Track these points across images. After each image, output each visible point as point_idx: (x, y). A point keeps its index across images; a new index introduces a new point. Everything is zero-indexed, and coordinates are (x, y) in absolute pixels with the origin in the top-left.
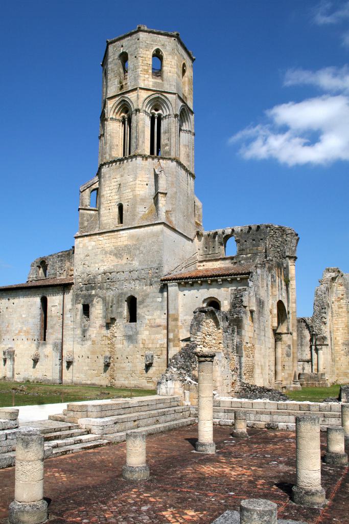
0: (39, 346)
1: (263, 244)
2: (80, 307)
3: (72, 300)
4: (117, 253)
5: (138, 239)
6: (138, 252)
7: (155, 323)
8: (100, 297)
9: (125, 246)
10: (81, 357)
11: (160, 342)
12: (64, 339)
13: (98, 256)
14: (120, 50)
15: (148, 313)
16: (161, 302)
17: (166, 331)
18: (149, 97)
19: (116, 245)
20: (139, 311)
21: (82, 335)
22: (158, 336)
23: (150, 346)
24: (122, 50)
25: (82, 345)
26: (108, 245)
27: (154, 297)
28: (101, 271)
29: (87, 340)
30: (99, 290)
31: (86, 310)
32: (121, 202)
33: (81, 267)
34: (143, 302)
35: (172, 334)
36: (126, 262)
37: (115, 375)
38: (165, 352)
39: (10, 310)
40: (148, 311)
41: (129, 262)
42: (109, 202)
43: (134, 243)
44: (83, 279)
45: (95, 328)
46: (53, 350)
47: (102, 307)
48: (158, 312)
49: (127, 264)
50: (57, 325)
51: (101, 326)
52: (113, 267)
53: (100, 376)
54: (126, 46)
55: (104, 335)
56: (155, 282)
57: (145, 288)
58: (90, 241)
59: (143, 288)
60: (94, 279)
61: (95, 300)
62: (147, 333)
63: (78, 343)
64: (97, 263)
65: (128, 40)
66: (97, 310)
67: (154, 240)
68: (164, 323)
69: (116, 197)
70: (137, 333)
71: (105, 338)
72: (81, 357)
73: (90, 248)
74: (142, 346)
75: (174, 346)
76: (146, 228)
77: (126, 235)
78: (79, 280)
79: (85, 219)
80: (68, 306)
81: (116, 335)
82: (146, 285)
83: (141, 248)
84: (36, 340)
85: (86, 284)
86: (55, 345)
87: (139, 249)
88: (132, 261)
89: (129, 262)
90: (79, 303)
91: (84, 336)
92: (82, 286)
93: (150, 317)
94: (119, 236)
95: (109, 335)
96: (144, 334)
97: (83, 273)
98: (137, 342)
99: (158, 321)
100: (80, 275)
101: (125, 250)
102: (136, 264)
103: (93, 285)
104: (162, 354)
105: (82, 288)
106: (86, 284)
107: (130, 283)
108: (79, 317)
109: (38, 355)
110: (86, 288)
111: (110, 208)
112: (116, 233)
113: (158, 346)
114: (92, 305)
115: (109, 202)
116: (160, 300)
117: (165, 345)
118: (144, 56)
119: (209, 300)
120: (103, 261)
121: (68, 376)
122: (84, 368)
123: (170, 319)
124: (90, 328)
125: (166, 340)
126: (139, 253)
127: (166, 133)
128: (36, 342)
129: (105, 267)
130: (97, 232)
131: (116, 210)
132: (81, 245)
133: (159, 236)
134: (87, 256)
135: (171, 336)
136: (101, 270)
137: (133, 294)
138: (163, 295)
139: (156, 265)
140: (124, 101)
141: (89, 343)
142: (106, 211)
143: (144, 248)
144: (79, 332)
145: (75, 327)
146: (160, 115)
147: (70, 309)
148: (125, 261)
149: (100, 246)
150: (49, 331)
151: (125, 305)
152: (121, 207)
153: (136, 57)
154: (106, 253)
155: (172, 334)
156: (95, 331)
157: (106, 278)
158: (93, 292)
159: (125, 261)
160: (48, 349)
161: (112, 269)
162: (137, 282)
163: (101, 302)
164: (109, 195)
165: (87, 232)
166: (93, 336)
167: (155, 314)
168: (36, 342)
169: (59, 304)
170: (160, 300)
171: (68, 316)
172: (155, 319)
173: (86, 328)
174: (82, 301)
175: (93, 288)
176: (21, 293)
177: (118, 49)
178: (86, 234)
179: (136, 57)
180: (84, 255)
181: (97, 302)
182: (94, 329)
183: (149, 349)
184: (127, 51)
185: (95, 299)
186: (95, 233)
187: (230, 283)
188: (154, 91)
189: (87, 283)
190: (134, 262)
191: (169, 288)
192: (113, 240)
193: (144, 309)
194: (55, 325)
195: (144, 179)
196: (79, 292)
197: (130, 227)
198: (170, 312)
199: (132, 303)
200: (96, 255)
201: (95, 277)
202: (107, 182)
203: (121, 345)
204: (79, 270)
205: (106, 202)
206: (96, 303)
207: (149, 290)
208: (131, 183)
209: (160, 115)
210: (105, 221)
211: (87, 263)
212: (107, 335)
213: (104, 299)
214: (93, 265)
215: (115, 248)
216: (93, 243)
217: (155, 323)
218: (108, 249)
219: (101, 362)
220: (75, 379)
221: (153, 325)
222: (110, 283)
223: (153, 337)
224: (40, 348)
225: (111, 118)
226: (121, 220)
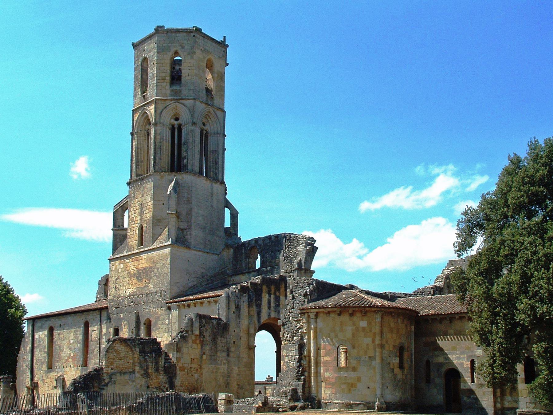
4: (140, 275)
27: (164, 319)
39: (62, 336)
83: (156, 271)
128: (80, 368)
134: (118, 278)
150: (90, 356)
151: (143, 328)
168: (80, 368)
216: (122, 266)
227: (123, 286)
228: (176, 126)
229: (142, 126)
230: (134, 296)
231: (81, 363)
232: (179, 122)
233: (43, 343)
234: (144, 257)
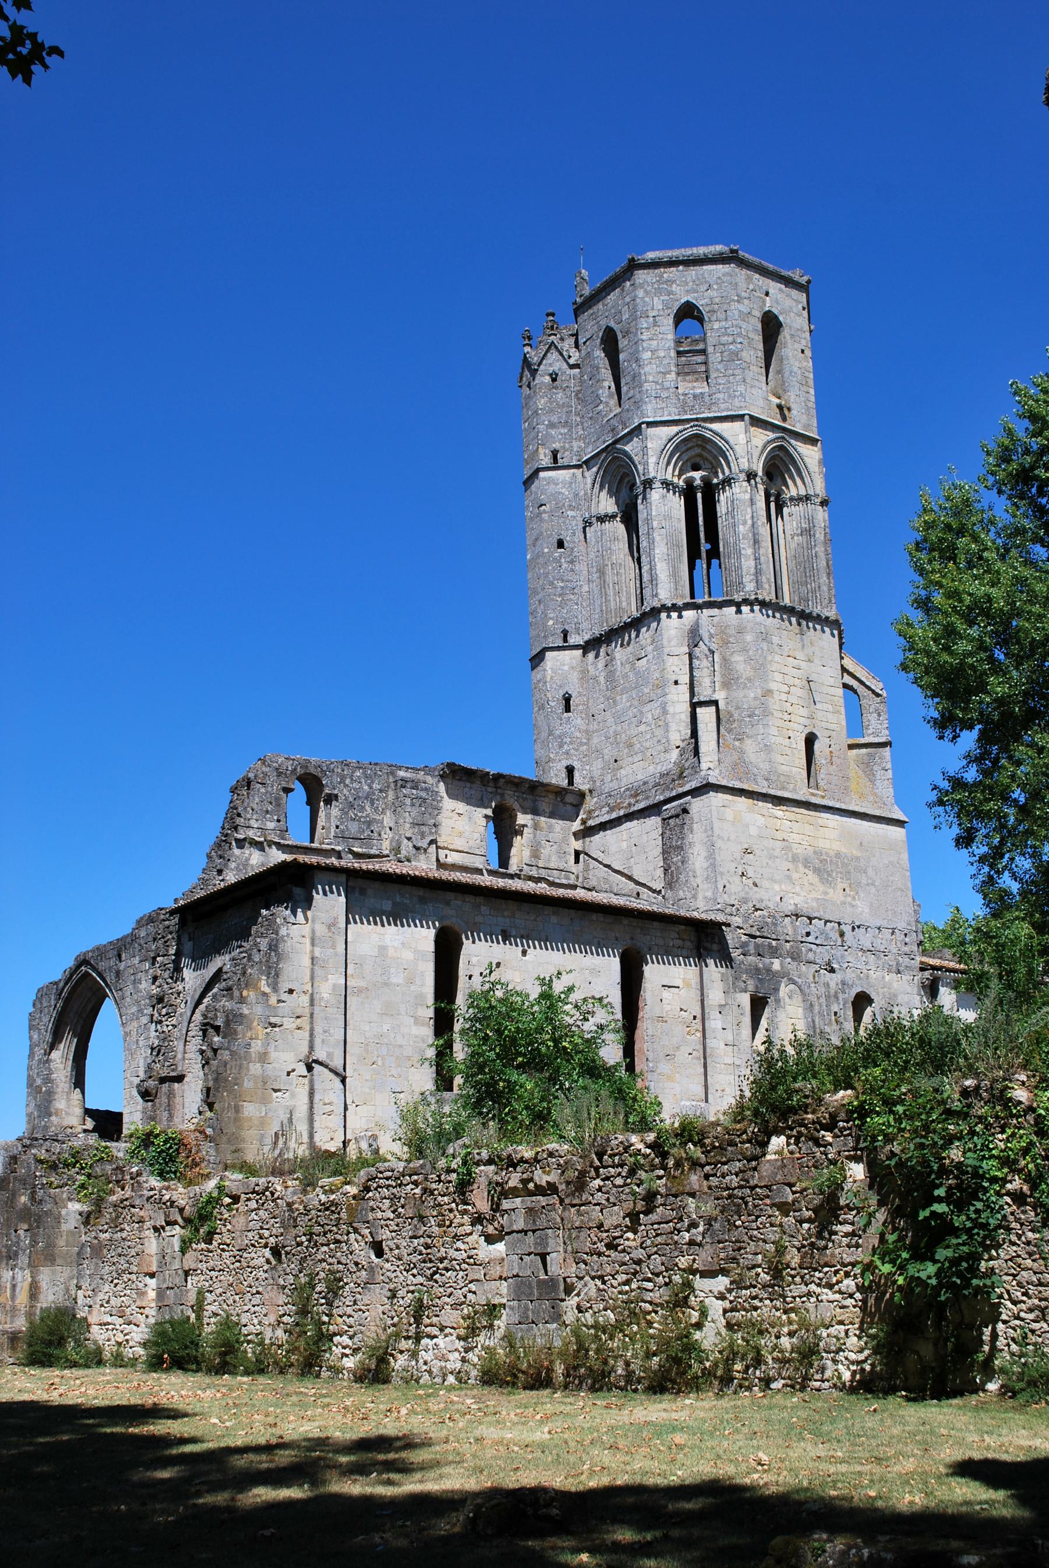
2: (745, 1000)
4: (822, 866)
8: (795, 983)
9: (838, 855)
30: (789, 960)
42: (787, 717)
47: (800, 1011)
50: (685, 1050)
52: (815, 904)
57: (887, 978)
59: (883, 977)
61: (784, 990)
64: (775, 881)
69: (804, 712)
73: (753, 831)
80: (715, 995)
83: (870, 871)
89: (849, 899)
100: (736, 902)
103: (774, 943)
110: (757, 946)
114: (778, 1001)
129: (798, 900)
140: (781, 448)
149: (779, 835)
154: (795, 859)
163: (798, 999)
171: (715, 1023)
175: (774, 952)
176: (554, 919)
185: (783, 985)
189: (758, 934)
192: (808, 830)
205: (780, 716)
207: (895, 985)
214: (765, 884)
215: (815, 852)
216: (761, 820)
218: (799, 850)
233: (410, 981)
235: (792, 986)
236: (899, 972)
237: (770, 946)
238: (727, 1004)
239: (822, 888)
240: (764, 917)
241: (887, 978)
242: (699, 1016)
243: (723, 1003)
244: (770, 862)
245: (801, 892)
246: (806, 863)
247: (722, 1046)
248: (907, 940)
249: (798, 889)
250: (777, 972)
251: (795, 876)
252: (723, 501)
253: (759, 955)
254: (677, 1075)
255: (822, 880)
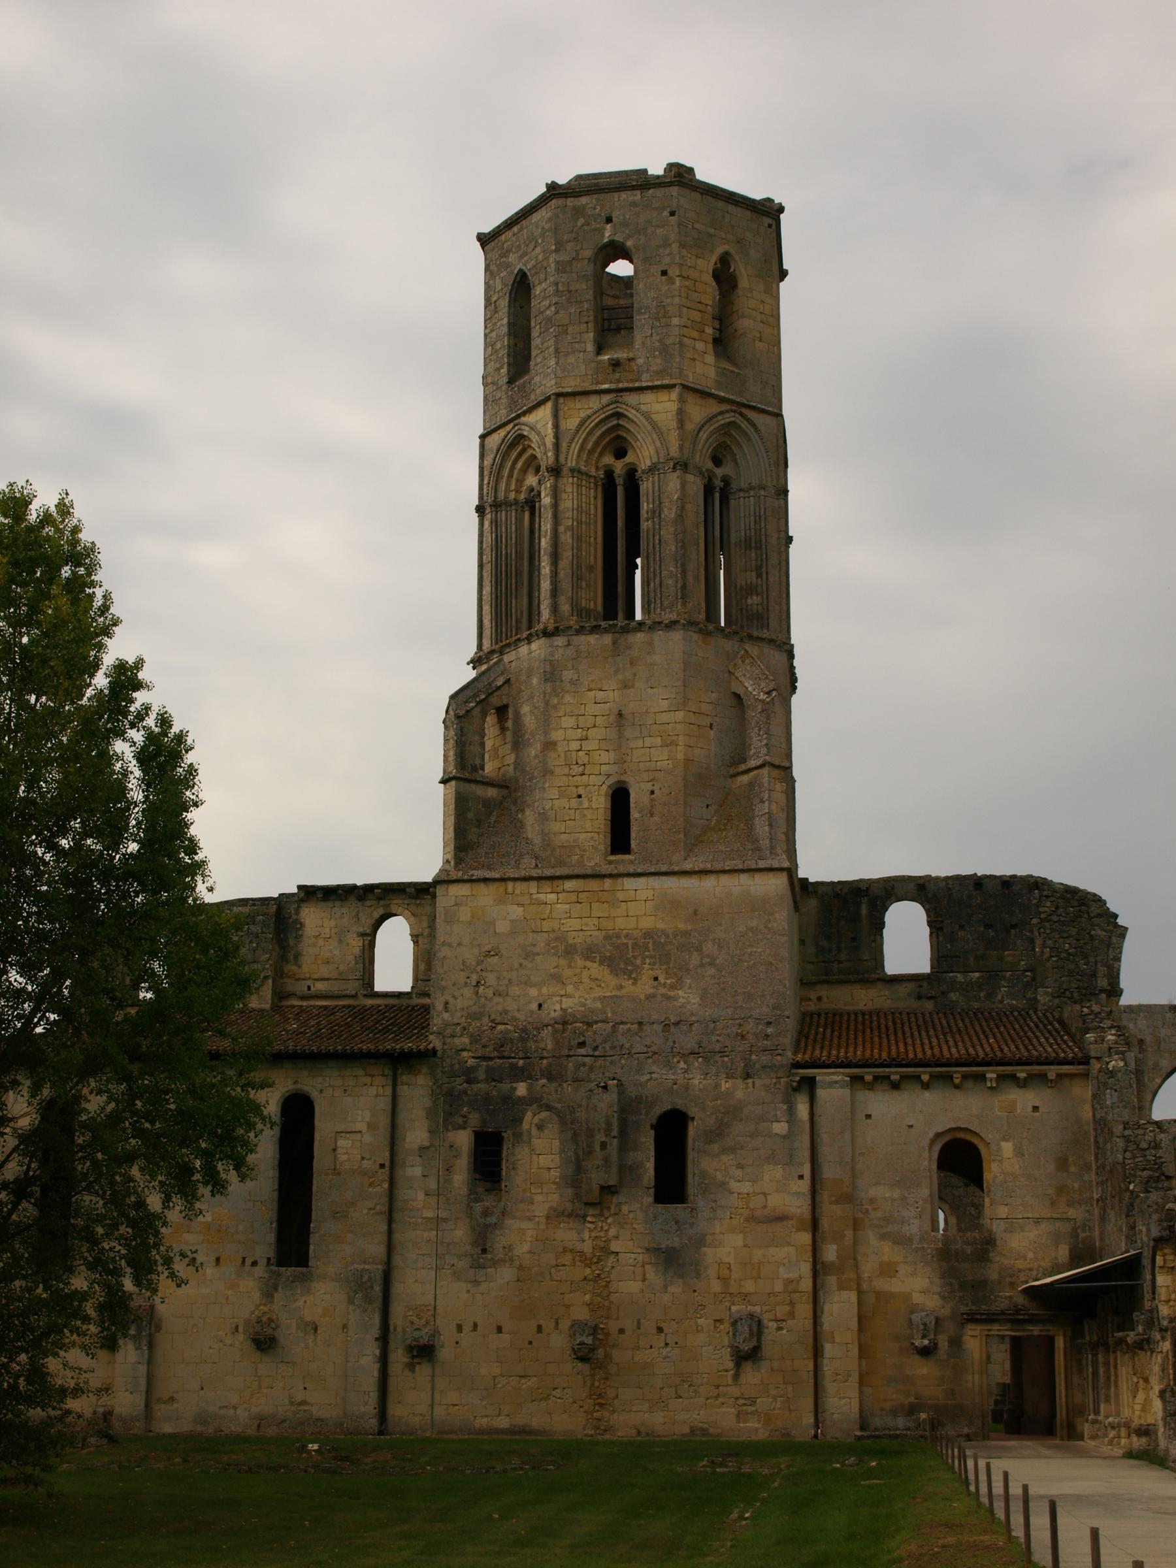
0: (276, 1290)
1: (1019, 942)
2: (463, 1139)
3: (431, 1114)
4: (618, 955)
5: (695, 912)
6: (695, 960)
7: (765, 1207)
8: (549, 1108)
9: (648, 934)
10: (467, 1328)
11: (784, 1273)
12: (397, 1260)
13: (539, 959)
14: (601, 232)
15: (739, 1173)
16: (784, 1137)
17: (806, 1238)
18: (710, 419)
19: (609, 924)
20: (703, 1163)
21: (475, 1244)
22: (778, 1253)
23: (749, 1286)
24: (608, 233)
25: (476, 1283)
26: (575, 923)
28: (553, 1015)
29: (495, 1264)
30: (544, 1081)
31: (488, 1161)
32: (623, 778)
33: (468, 992)
34: (716, 1134)
35: (835, 1247)
36: (652, 991)
37: (611, 1393)
38: (804, 1310)
40: (740, 1166)
41: (662, 990)
42: (577, 770)
43: (681, 926)
44: (475, 1039)
45: (530, 1219)
46: (351, 1301)
48: (777, 1172)
49: (654, 996)
51: (556, 1216)
52: (598, 1005)
53: (547, 1398)
54: (625, 224)
55: (569, 1245)
56: (764, 1067)
57: (725, 1086)
58: (500, 902)
59: (718, 1086)
60: (522, 1039)
61: (529, 1119)
62: (737, 1240)
63: (457, 1276)
65: (634, 204)
66: (538, 1157)
67: (755, 923)
68: (799, 1206)
70: (700, 1242)
71: (567, 1259)
72: (467, 1328)
73: (502, 927)
74: (716, 1287)
75: (841, 1288)
76: (725, 880)
77: (648, 894)
78: (457, 1041)
79: (470, 815)
80: (416, 1135)
81: (614, 1246)
82: (730, 1076)
83: (709, 948)
84: (262, 1263)
85: (490, 1059)
86: (357, 1285)
87: (699, 949)
88: (672, 987)
89: (662, 990)
90: (464, 1128)
91: (484, 1251)
92: (471, 1062)
93: (746, 1187)
94: (621, 896)
95: (587, 1247)
96: (726, 1246)
97: (477, 1016)
98: (698, 1275)
99: (777, 1201)
101: (647, 949)
102: (688, 998)
103: (521, 1062)
104: (792, 1315)
105: (472, 1069)
106: (490, 1059)
107: (668, 1065)
108: (461, 1177)
109: (271, 1320)
110: (489, 1070)
111: (581, 791)
112: (608, 883)
113: (779, 1287)
114: (518, 1136)
115: (577, 770)
116: (780, 1128)
117: (807, 1284)
118: (693, 274)
119: (947, 1138)
120: (557, 978)
121: (418, 1402)
122: (484, 1371)
123: (825, 1197)
124: (509, 1222)
125: (806, 1268)
126: (702, 965)
127: (748, 547)
128: (260, 1271)
129: (567, 1003)
130: (534, 873)
131: (601, 803)
132: (464, 914)
133: (772, 914)
135: (830, 1253)
136: (554, 1009)
137: (680, 1103)
138: (791, 1110)
139: (765, 1010)
140: (619, 415)
141: (506, 1274)
142: (564, 803)
143: (720, 947)
144: (460, 1233)
145: (443, 1215)
146: (726, 481)
147: (422, 1149)
148: (645, 987)
149: (546, 926)
150: (323, 1226)
151: (648, 1140)
152: (620, 798)
153: (664, 273)
154: (570, 951)
155: (835, 1247)
156: (530, 1233)
157: (574, 1043)
158: (522, 1089)
159: (645, 987)
160: (322, 1298)
161: (593, 1011)
162: (697, 1063)
164: (575, 745)
165: (489, 868)
166: (522, 1249)
167: (766, 1177)
169: (371, 1126)
170: (780, 1128)
171: (413, 1170)
172: (765, 1195)
173: (493, 1220)
174: (475, 1119)
175: (518, 1074)
177: (594, 225)
178: (488, 874)
179: (664, 273)
180: (476, 951)
181: (540, 1127)
182: (524, 1225)
183: (745, 1297)
184: (629, 243)
185: (529, 1114)
186: (523, 873)
187: (1019, 1087)
188: (722, 400)
190: (681, 993)
191: (821, 1093)
192: (599, 910)
193: (725, 1158)
194: (353, 1204)
195: (706, 708)
196: (459, 1084)
197: (664, 868)
198: (829, 1172)
199: (672, 1130)
200: (529, 955)
201: (525, 1034)
202: (568, 698)
203: (633, 1279)
204: (460, 1003)
205: (566, 771)
206: (534, 1131)
207: (739, 1094)
208: (664, 718)
209: (726, 481)
210: (564, 837)
211: (491, 978)
212: (579, 1246)
213: (566, 1119)
214: (515, 990)
216: (517, 912)
217: (765, 1207)
219: (559, 1341)
220: (440, 1411)
221: (758, 1213)
222: (587, 1060)
223: (758, 1254)
224: (279, 1296)
225: (572, 470)
226: (620, 840)
227: (528, 983)
228: (718, 483)
229: (591, 452)
230: (589, 1024)
231: (265, 1245)
232: (726, 470)
234: (642, 895)
235: (545, 1114)
236: (748, 1076)
237: (514, 1067)
238: (432, 1146)
239: (613, 981)
240: (507, 1031)
241: (725, 1086)
242: (387, 1164)
243: (427, 1144)
244: (525, 962)
245: (582, 991)
246: (589, 953)
247: (421, 1196)
248: (770, 1030)
249: (570, 989)
250: (520, 1099)
251: (567, 973)
252: (645, 487)
253: (494, 1080)
254: (350, 1235)
255: (615, 972)
